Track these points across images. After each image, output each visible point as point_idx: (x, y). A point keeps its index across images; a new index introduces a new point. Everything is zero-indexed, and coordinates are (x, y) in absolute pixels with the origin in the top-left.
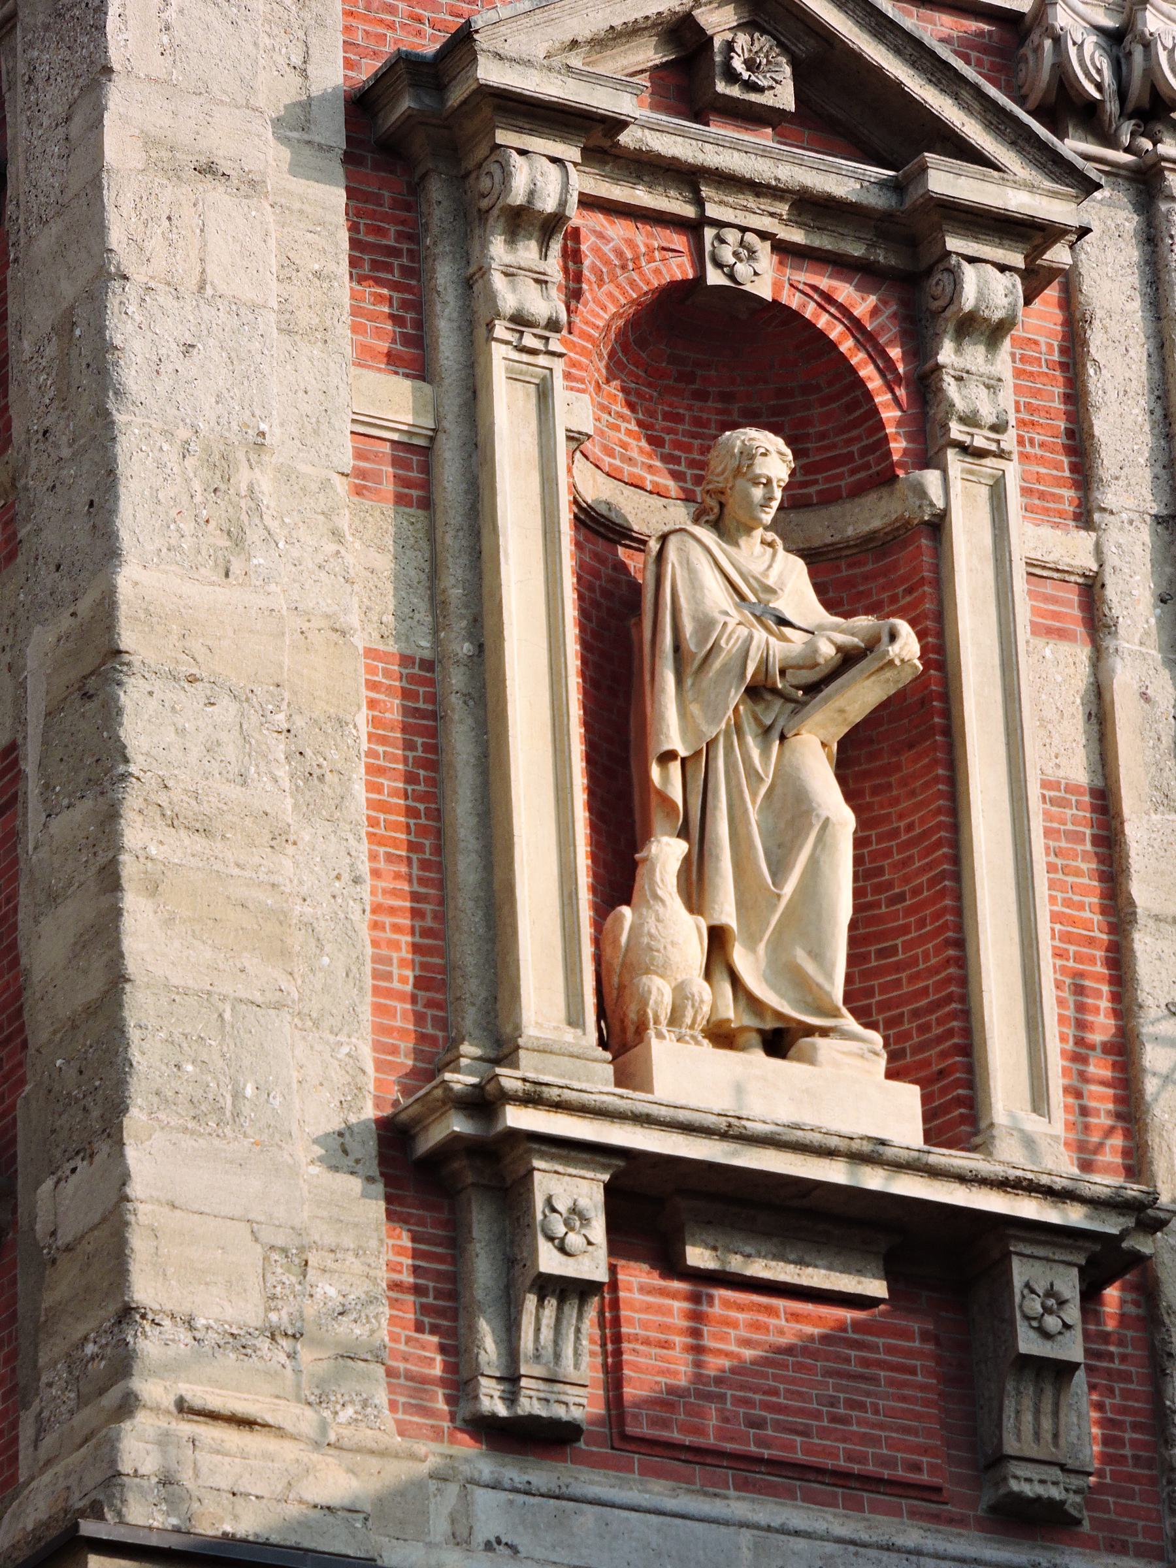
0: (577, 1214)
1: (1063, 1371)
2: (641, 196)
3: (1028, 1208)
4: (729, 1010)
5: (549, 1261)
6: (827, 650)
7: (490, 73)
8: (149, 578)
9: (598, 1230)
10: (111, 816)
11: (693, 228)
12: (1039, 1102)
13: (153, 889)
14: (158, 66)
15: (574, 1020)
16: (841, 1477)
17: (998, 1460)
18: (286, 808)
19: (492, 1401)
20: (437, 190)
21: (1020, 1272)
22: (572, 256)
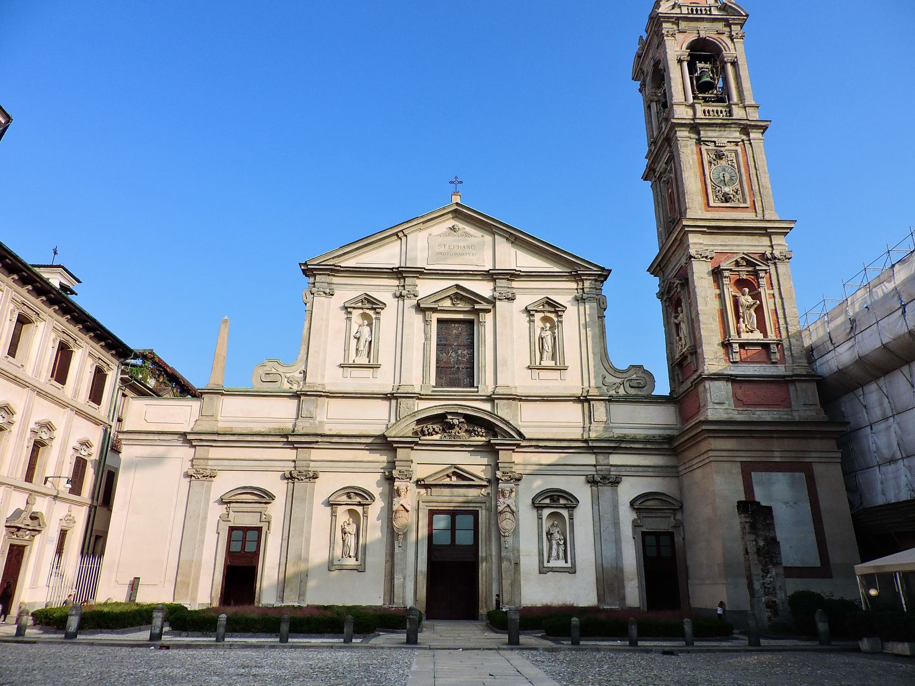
0: (736, 347)
1: (775, 352)
2: (735, 273)
3: (771, 342)
4: (747, 330)
5: (734, 351)
6: (752, 303)
7: (721, 268)
8: (701, 308)
9: (738, 348)
10: (699, 325)
11: (739, 275)
12: (772, 333)
13: (703, 329)
14: (697, 271)
15: (735, 333)
16: (759, 362)
17: (771, 359)
18: (712, 322)
19: (732, 360)
20: (719, 276)
21: (771, 346)
22: (730, 278)
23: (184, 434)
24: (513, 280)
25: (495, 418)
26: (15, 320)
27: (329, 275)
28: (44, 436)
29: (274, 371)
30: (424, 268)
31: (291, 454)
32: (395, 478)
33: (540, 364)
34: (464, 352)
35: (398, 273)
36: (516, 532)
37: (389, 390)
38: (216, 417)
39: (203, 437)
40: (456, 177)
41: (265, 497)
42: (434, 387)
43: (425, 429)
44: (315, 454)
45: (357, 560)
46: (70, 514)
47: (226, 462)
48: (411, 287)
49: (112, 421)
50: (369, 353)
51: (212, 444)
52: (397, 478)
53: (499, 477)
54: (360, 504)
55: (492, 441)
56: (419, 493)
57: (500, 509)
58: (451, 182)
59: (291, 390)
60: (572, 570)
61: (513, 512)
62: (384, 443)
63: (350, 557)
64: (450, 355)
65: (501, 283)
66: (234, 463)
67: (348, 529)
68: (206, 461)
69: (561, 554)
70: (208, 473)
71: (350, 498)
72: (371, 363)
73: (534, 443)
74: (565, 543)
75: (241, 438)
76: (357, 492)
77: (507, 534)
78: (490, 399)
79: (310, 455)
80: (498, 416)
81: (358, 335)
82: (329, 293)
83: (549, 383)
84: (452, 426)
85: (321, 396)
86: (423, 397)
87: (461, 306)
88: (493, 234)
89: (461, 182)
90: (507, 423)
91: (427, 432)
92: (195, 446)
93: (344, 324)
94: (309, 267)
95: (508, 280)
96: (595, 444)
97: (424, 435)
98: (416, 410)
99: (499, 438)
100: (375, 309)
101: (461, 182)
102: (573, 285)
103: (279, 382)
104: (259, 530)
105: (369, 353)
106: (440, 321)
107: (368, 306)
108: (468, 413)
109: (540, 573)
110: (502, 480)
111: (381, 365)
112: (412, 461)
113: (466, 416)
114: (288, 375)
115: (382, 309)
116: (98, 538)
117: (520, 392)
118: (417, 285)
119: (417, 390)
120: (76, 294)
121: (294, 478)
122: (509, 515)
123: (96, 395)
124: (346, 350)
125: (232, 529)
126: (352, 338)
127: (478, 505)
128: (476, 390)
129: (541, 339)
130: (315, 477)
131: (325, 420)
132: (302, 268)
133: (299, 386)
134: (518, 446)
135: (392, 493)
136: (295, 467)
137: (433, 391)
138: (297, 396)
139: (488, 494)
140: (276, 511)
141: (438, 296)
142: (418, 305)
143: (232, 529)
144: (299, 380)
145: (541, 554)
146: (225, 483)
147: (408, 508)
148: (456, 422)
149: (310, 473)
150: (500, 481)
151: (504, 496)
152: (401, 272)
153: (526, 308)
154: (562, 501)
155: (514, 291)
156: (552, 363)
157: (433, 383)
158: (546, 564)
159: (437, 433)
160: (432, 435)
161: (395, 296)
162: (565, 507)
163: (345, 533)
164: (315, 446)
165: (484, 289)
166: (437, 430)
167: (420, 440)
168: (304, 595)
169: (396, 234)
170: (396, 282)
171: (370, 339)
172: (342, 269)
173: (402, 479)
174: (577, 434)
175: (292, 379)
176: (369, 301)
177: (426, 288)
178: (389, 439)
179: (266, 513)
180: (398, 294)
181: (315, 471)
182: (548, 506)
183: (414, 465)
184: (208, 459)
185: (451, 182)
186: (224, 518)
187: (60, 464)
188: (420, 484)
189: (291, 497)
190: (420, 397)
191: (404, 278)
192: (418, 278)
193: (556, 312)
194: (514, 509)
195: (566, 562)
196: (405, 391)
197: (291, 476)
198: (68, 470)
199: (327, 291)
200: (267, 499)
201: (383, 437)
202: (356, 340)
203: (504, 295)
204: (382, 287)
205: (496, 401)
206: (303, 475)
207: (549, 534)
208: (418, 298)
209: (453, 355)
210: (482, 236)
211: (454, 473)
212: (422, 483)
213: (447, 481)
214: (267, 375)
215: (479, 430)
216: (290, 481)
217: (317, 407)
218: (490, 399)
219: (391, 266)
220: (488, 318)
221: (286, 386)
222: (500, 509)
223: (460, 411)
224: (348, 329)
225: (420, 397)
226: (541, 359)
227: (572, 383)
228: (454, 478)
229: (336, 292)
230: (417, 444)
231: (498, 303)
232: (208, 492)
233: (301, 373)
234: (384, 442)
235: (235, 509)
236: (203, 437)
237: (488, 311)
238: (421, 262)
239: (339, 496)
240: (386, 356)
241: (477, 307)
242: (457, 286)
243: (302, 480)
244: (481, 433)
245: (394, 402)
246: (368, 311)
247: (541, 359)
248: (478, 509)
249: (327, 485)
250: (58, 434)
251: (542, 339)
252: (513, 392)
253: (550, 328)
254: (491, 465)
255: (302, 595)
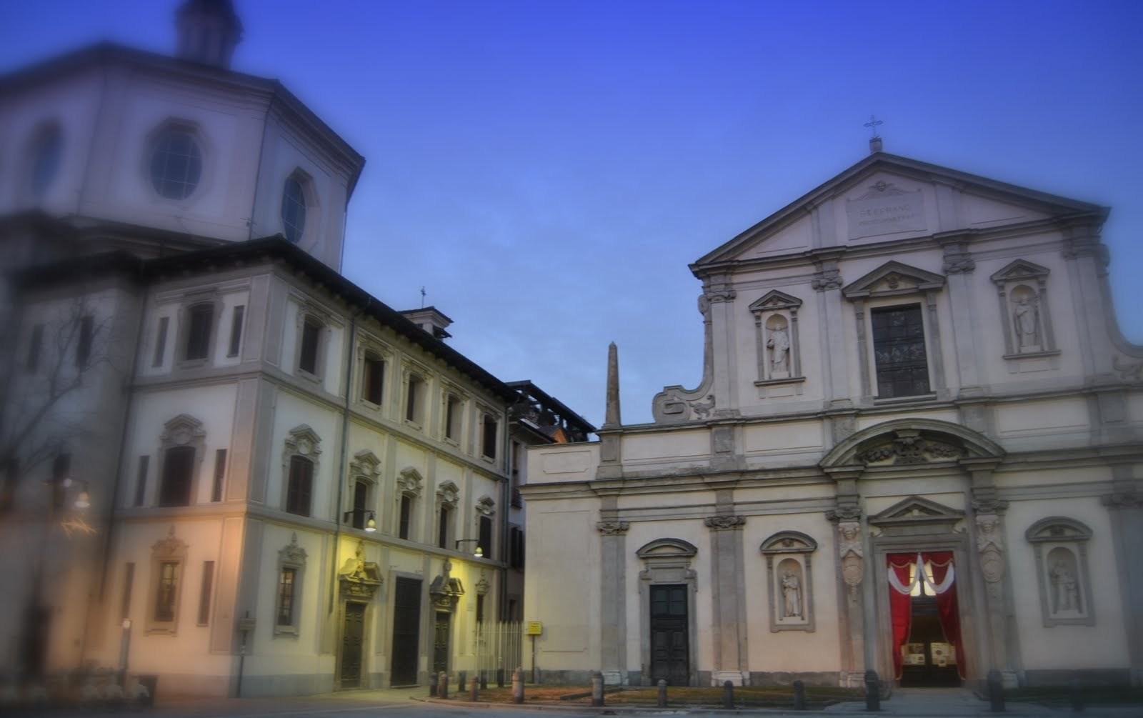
23: (587, 483)
24: (968, 244)
25: (963, 432)
26: (407, 382)
27: (725, 274)
28: (450, 500)
29: (676, 400)
30: (845, 246)
31: (710, 497)
32: (839, 518)
33: (1020, 351)
34: (912, 348)
35: (815, 257)
36: (1006, 575)
37: (819, 408)
38: (620, 461)
39: (608, 486)
40: (873, 117)
41: (688, 551)
42: (876, 398)
43: (870, 454)
44: (739, 496)
45: (803, 619)
46: (483, 578)
47: (637, 513)
48: (832, 273)
49: (508, 473)
50: (788, 364)
51: (619, 492)
52: (842, 517)
53: (975, 507)
54: (799, 552)
55: (962, 462)
56: (872, 534)
57: (981, 547)
58: (867, 125)
59: (700, 421)
60: (1090, 622)
61: (999, 552)
62: (822, 473)
63: (794, 615)
64: (893, 354)
65: (955, 250)
66: (645, 513)
67: (788, 583)
68: (615, 513)
69: (1073, 600)
70: (617, 525)
71: (788, 546)
72: (793, 375)
73: (1020, 460)
74: (1077, 588)
75: (651, 483)
76: (793, 537)
77: (993, 580)
78: (956, 405)
79: (732, 496)
80: (965, 428)
81: (771, 343)
82: (729, 296)
83: (1035, 375)
84: (906, 447)
85: (735, 425)
86: (863, 413)
87: (902, 285)
88: (934, 183)
89: (880, 122)
90: (979, 435)
91: (873, 458)
92: (600, 496)
93: (752, 334)
94: (701, 267)
95: (960, 244)
96: (1110, 453)
97: (872, 461)
98: (857, 431)
99: (972, 455)
100: (788, 308)
101: (880, 122)
102: (1056, 237)
103: (684, 413)
104: (683, 588)
105: (788, 364)
106: (875, 312)
107: (781, 304)
108: (925, 428)
109: (1045, 627)
110: (981, 511)
111: (804, 378)
112: (859, 496)
113: (924, 434)
114: (694, 403)
115: (798, 307)
116: (512, 602)
117: (996, 391)
118: (838, 270)
119: (857, 403)
120: (450, 336)
121: (717, 525)
122: (993, 556)
123: (489, 449)
124: (760, 364)
125: (654, 588)
126: (765, 348)
127: (953, 544)
128: (934, 396)
129: (1018, 317)
130: (739, 523)
131: (746, 454)
132: (693, 270)
133: (708, 415)
134: (999, 464)
135: (839, 535)
136: (717, 512)
137: (876, 404)
138: (709, 426)
139: (964, 530)
140: (702, 565)
141: (870, 281)
142: (843, 295)
143: (654, 588)
144: (707, 407)
145: (1043, 600)
146: (640, 535)
147: (860, 553)
148: (909, 441)
149: (734, 518)
150: (978, 513)
151: (984, 531)
152: (816, 256)
153: (991, 278)
154: (1068, 533)
155: (972, 257)
156: (1036, 349)
157: (875, 393)
158: (1052, 616)
159: (887, 457)
160: (882, 460)
161: (815, 288)
162: (1073, 540)
163: (785, 588)
164: (738, 486)
165: (930, 261)
166: (886, 453)
167: (866, 467)
168: (746, 660)
169: (804, 208)
170: (812, 269)
171: (786, 347)
172: (741, 264)
173: (848, 518)
174: (1081, 439)
175: (698, 408)
176: (780, 299)
177: (852, 271)
178: (826, 471)
179: (690, 568)
180: (815, 284)
181: (741, 516)
182: (1048, 541)
183: (862, 499)
184: (619, 510)
185: (867, 125)
186: (643, 577)
187: (467, 526)
188: (874, 521)
189: (716, 549)
190: (859, 413)
191: (821, 262)
192: (838, 260)
193: (1035, 277)
194: (1000, 546)
195: (1080, 611)
196: (840, 408)
197: (712, 523)
198: (474, 533)
199: (726, 294)
200: (689, 552)
201: (819, 467)
202: (770, 351)
203: (957, 265)
204: (793, 279)
205: (963, 408)
206: (724, 522)
207: (1054, 577)
208: (842, 288)
209: (898, 353)
210: (919, 190)
211: (915, 506)
212: (875, 521)
213: (908, 517)
214: (669, 407)
215: (942, 448)
216: (713, 529)
217: (732, 438)
218: (956, 405)
219: (802, 250)
220: (942, 302)
221: (694, 417)
222: (981, 547)
223: (914, 427)
224: (759, 339)
225: (859, 413)
226: (1020, 344)
227: (1071, 369)
228: (916, 512)
229: (740, 294)
230: (862, 472)
231: (952, 279)
232: (621, 550)
233: (709, 399)
234: (820, 474)
235: (654, 566)
236: (608, 486)
237: (937, 290)
238: (843, 237)
239: (774, 544)
240: (811, 366)
241: (923, 286)
242: (892, 263)
243: (726, 527)
244: (945, 453)
245: (827, 423)
246: (782, 313)
247: (1020, 344)
248: (951, 549)
249: (757, 531)
250: (461, 494)
251: (1019, 317)
252: (986, 393)
253: (1029, 300)
254: (963, 492)
255: (741, 662)
